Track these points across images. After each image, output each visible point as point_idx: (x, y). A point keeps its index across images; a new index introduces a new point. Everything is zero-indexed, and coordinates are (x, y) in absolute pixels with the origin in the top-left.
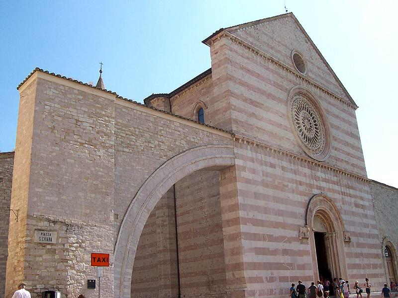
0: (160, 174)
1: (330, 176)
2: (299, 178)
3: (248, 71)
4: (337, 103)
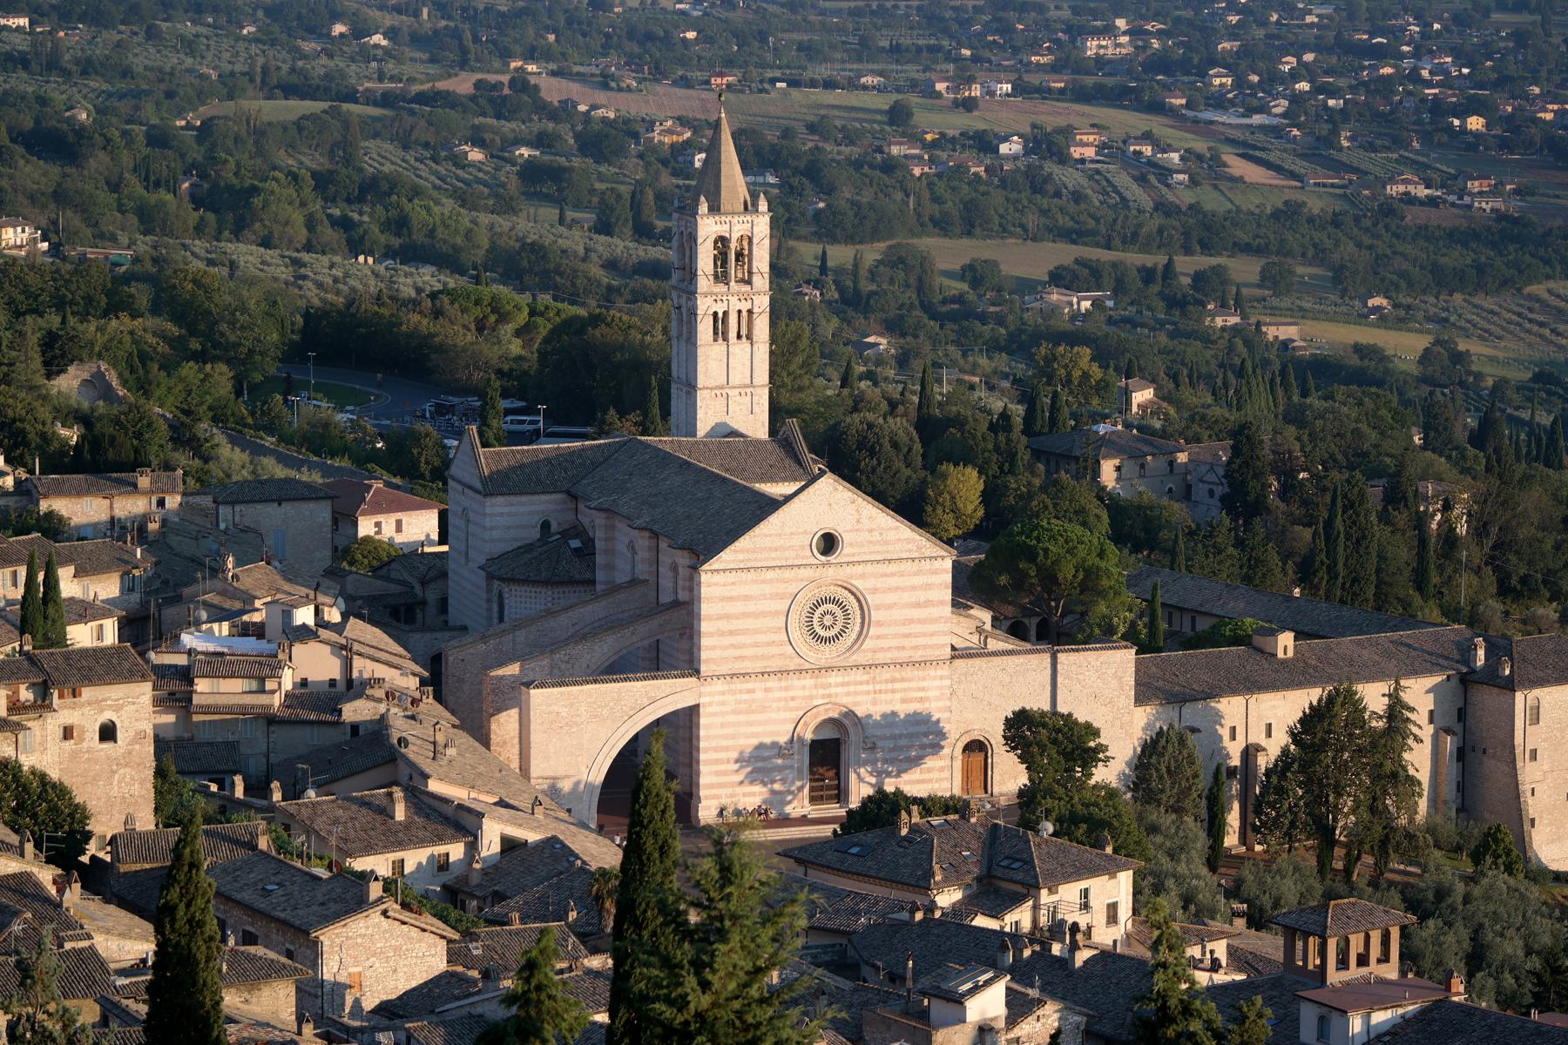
0: (622, 730)
1: (860, 675)
2: (791, 694)
3: (731, 599)
4: (908, 566)
